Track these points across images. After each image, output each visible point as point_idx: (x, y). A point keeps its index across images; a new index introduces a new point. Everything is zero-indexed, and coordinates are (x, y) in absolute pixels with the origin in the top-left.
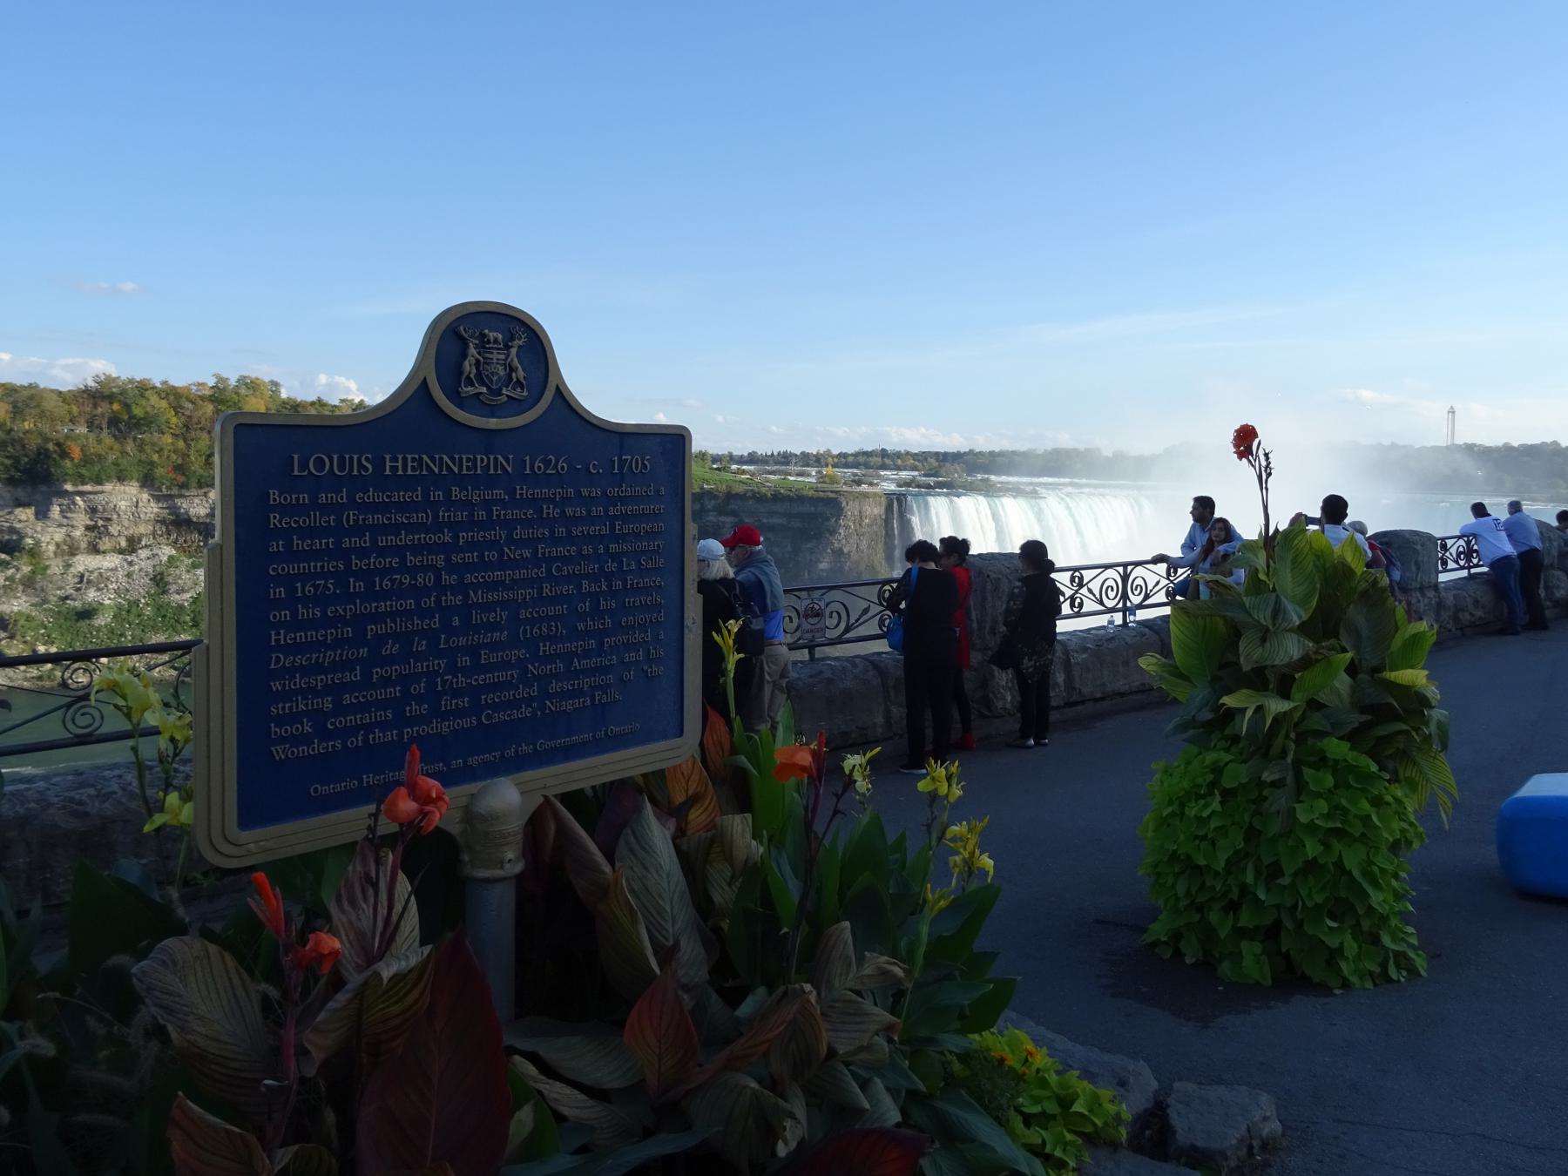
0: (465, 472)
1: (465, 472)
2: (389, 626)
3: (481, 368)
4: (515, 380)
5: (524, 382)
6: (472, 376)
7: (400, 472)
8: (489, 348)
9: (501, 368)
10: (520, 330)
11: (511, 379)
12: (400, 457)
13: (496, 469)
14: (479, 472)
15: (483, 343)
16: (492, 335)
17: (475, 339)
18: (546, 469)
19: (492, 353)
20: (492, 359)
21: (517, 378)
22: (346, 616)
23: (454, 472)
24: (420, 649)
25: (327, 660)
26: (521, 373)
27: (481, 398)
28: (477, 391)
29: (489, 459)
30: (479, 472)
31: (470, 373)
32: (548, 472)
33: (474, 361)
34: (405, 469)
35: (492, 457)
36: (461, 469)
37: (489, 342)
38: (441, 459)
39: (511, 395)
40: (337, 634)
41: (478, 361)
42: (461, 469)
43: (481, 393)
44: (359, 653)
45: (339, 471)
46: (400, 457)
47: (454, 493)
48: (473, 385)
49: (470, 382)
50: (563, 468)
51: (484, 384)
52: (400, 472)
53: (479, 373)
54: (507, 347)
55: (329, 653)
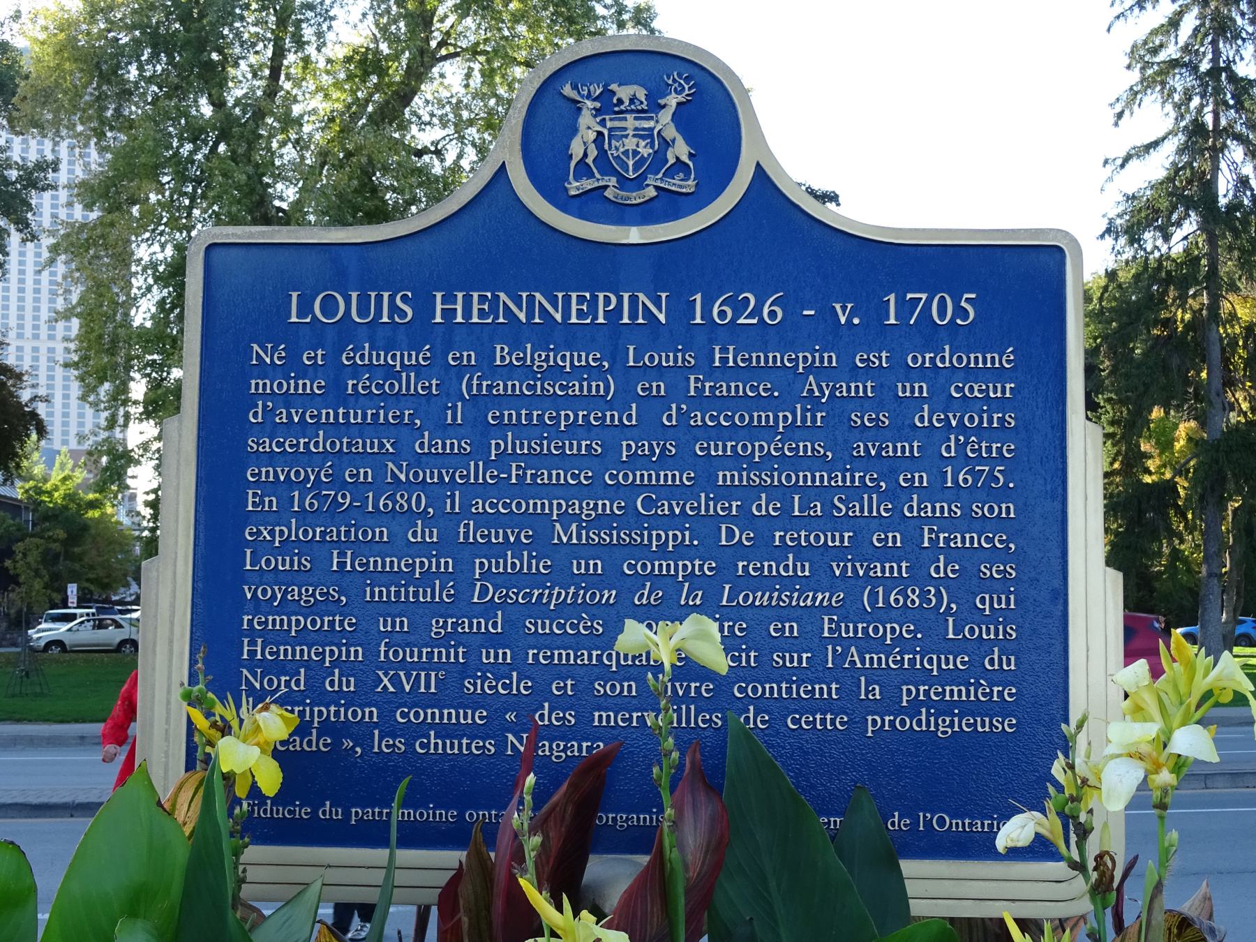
0: (574, 320)
1: (574, 320)
2: (509, 562)
3: (606, 147)
4: (672, 161)
5: (691, 165)
6: (589, 161)
7: (459, 319)
8: (621, 112)
9: (643, 143)
10: (680, 76)
11: (667, 161)
12: (460, 295)
13: (634, 315)
14: (601, 320)
15: (607, 105)
16: (624, 93)
17: (595, 100)
18: (736, 315)
19: (625, 119)
20: (625, 129)
21: (677, 158)
22: (273, 541)
23: (520, 321)
24: (802, 604)
25: (554, 602)
26: (681, 150)
27: (606, 194)
28: (596, 185)
29: (620, 299)
30: (601, 320)
31: (585, 155)
32: (741, 321)
33: (592, 136)
34: (467, 313)
35: (626, 296)
36: (566, 315)
37: (620, 101)
38: (531, 299)
39: (662, 185)
40: (430, 566)
41: (600, 134)
42: (566, 314)
43: (606, 187)
44: (602, 596)
45: (359, 316)
46: (460, 295)
47: (498, 354)
48: (591, 175)
49: (583, 170)
50: (772, 314)
51: (615, 172)
52: (459, 319)
53: (602, 153)
54: (656, 107)
55: (557, 590)
